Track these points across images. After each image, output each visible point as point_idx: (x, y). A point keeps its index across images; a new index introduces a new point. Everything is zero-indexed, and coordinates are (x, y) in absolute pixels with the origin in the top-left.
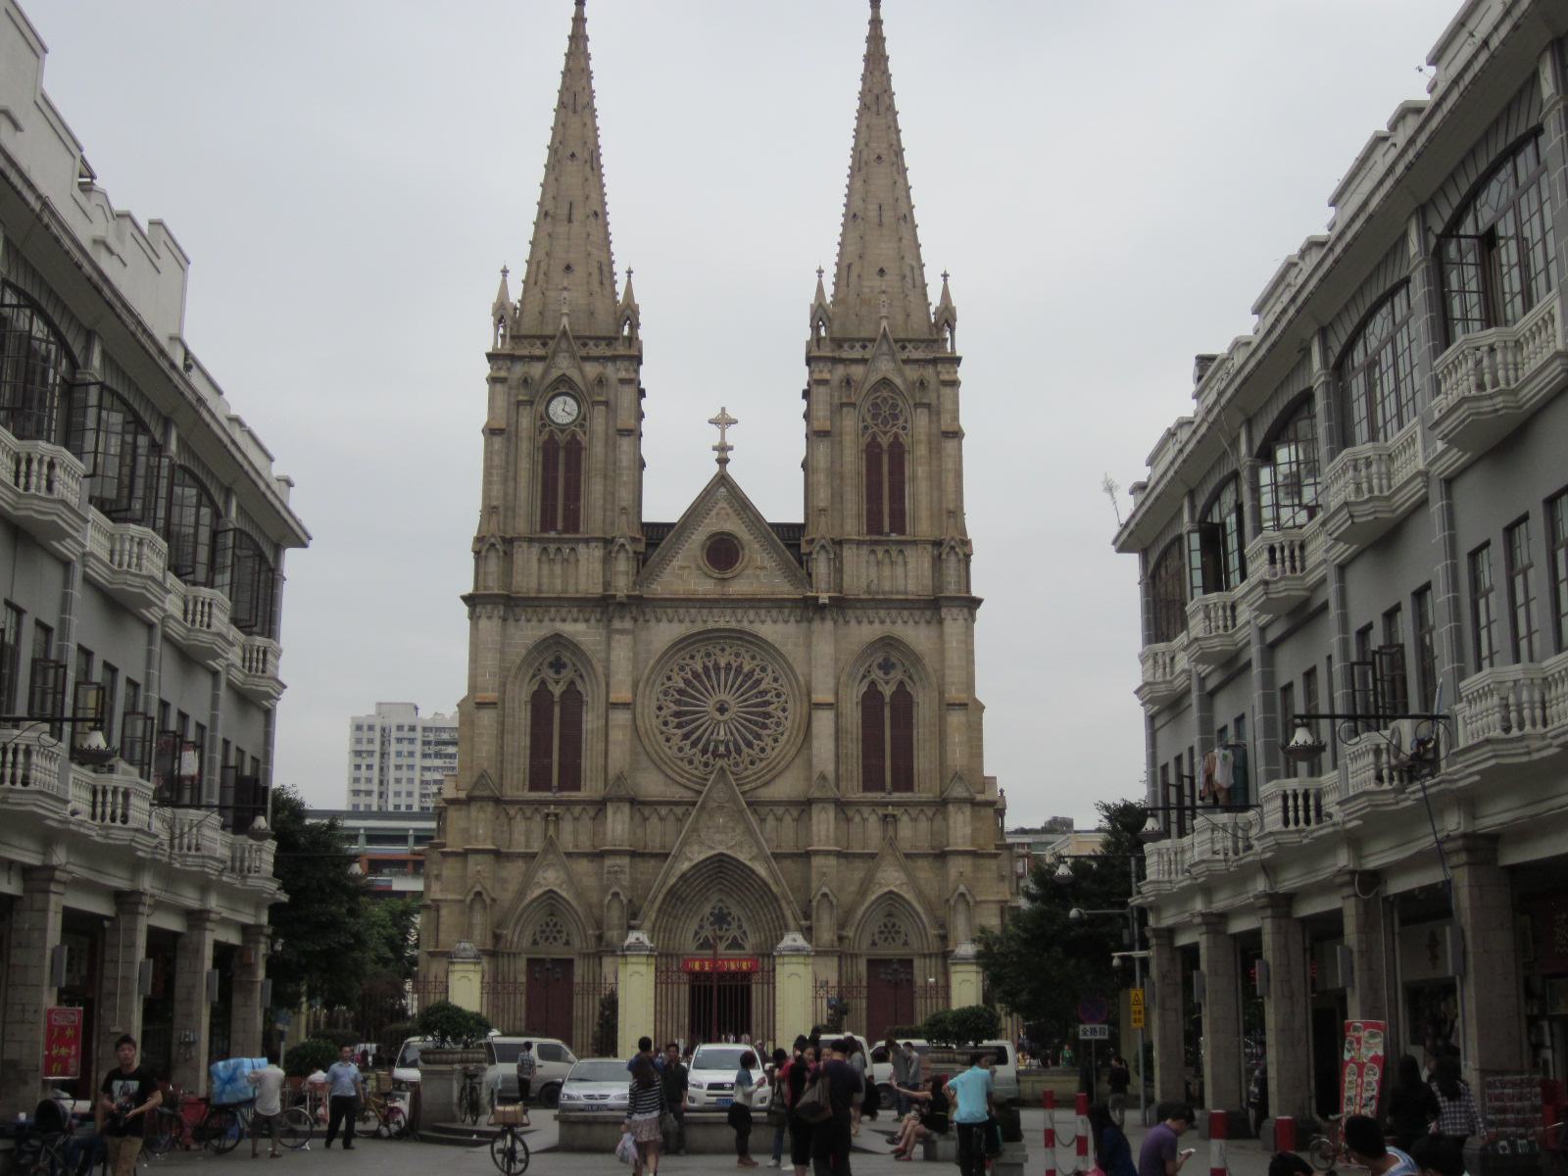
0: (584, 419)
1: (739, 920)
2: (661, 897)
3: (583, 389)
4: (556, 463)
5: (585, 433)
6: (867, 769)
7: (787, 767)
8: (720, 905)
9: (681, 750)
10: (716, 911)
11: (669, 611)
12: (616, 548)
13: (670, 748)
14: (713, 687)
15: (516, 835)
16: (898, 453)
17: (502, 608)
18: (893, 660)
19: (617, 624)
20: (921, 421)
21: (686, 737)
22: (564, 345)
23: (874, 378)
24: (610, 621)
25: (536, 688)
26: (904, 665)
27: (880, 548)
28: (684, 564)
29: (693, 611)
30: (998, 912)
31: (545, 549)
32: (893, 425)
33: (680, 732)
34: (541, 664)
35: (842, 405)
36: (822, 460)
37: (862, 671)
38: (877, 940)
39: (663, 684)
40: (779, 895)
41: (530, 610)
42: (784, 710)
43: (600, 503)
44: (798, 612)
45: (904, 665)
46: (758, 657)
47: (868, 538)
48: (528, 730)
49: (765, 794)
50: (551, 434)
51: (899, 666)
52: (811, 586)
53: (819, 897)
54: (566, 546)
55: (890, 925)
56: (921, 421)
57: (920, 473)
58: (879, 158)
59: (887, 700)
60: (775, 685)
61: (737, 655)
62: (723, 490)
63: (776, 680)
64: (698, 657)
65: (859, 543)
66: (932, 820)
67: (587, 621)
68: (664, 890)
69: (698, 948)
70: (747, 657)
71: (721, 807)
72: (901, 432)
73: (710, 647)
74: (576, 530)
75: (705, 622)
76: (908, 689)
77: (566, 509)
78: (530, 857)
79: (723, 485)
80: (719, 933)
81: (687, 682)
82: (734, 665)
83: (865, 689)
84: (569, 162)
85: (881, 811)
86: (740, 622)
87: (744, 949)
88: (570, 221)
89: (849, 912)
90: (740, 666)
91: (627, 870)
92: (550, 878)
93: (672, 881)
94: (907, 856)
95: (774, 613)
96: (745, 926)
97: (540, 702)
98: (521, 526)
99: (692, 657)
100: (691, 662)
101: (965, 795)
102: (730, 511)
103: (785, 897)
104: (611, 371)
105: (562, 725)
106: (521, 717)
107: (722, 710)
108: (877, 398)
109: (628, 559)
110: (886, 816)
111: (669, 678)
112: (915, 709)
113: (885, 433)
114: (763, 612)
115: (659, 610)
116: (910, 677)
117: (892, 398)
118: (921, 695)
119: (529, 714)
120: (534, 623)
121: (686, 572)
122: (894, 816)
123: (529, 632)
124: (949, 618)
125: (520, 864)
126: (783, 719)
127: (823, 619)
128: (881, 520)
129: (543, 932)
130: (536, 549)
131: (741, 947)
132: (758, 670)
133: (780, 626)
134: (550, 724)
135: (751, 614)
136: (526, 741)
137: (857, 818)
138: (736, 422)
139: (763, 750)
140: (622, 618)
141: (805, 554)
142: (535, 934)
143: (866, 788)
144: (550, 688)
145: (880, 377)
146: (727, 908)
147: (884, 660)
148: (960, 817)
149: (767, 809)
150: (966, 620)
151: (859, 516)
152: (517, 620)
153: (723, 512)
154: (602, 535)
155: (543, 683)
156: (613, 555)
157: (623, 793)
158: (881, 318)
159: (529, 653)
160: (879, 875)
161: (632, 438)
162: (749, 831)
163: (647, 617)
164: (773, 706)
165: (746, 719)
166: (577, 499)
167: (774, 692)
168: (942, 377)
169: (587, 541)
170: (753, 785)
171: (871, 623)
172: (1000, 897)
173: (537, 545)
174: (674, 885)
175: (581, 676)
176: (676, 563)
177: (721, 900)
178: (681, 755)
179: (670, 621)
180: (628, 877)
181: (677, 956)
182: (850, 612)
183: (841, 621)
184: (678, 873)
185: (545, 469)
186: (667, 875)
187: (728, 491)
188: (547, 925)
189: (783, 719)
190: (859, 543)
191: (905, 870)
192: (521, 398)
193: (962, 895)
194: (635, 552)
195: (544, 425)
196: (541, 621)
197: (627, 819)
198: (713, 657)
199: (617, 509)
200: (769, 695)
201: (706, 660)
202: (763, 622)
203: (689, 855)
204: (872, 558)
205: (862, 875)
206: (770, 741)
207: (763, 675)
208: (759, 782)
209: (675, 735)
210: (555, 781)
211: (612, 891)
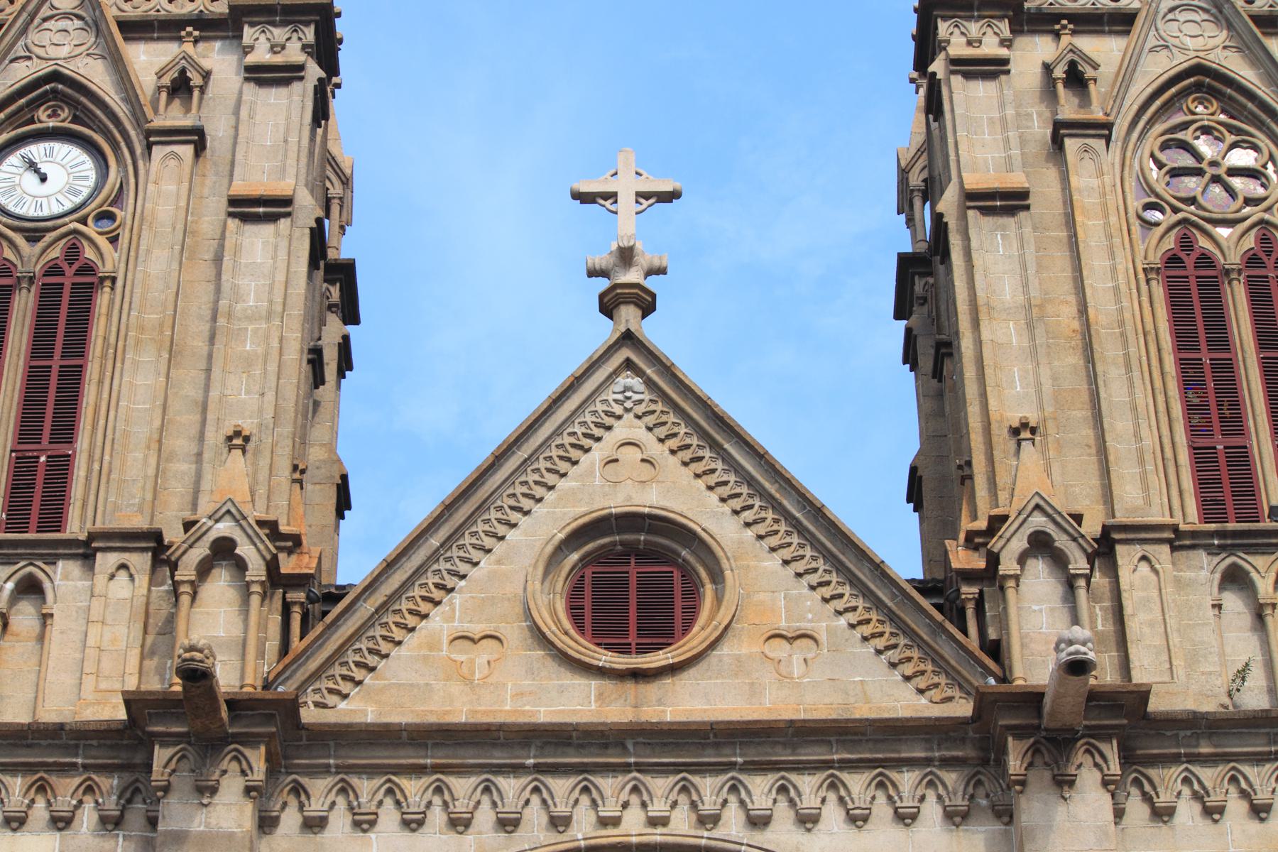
0: (118, 199)
3: (121, 109)
5: (114, 240)
11: (413, 788)
12: (201, 551)
23: (1157, 67)
24: (153, 822)
27: (1260, 561)
28: (477, 629)
29: (510, 786)
43: (143, 431)
44: (951, 777)
47: (1212, 527)
52: (1004, 679)
65: (1179, 540)
67: (61, 822)
74: (54, 517)
79: (628, 364)
86: (708, 820)
95: (857, 783)
102: (657, 451)
108: (1184, 126)
109: (245, 591)
114: (808, 785)
115: (366, 787)
117: (1232, 129)
127: (1064, 783)
135: (760, 788)
140: (206, 790)
141: (969, 576)
145: (1180, 62)
151: (1167, 464)
153: (631, 454)
154: (139, 522)
156: (186, 571)
161: (284, 223)
163: (316, 806)
166: (66, 430)
169: (85, 551)
176: (439, 623)
179: (413, 824)
182: (1168, 780)
183: (1136, 809)
187: (649, 383)
194: (272, 566)
199: (214, 437)
204: (1233, 602)
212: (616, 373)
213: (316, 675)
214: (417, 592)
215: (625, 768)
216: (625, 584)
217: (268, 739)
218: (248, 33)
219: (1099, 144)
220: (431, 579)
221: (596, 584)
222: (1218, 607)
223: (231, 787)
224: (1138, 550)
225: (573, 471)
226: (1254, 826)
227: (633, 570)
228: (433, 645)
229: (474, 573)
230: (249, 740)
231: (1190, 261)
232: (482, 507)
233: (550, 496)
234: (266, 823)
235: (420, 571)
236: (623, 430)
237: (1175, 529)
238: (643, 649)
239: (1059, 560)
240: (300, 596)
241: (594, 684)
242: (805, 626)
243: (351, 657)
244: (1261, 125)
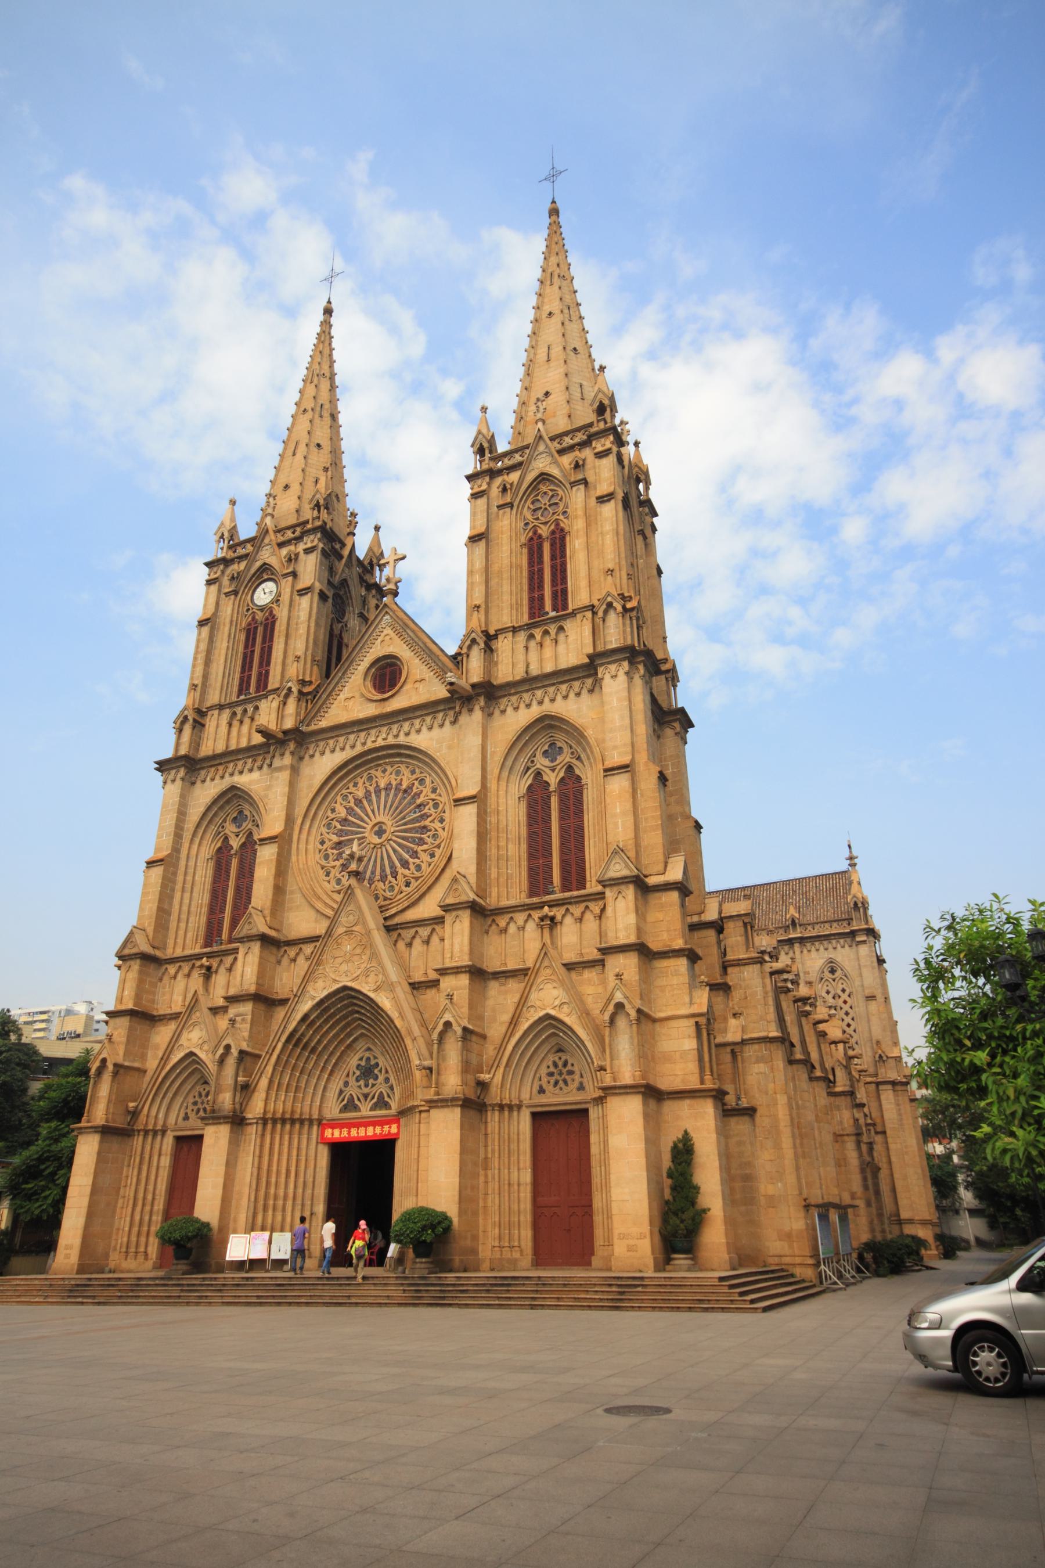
1: (387, 1072)
2: (280, 1046)
4: (254, 639)
6: (532, 873)
7: (437, 879)
8: (367, 1054)
9: (339, 881)
10: (363, 1063)
12: (285, 691)
13: (329, 882)
14: (373, 811)
15: (175, 997)
16: (559, 539)
17: (182, 772)
18: (559, 744)
19: (277, 763)
20: (577, 497)
21: (344, 866)
22: (266, 541)
23: (530, 477)
25: (219, 845)
26: (571, 747)
28: (350, 695)
30: (692, 1031)
31: (234, 714)
32: (554, 514)
33: (338, 863)
34: (225, 821)
35: (499, 507)
36: (479, 564)
37: (522, 762)
38: (544, 1086)
39: (327, 817)
40: (403, 1031)
41: (213, 769)
42: (442, 821)
45: (571, 747)
46: (417, 770)
48: (208, 886)
49: (412, 915)
50: (254, 618)
51: (566, 749)
53: (440, 1027)
54: (251, 705)
55: (560, 1064)
56: (577, 497)
57: (577, 545)
58: (550, 314)
59: (552, 788)
60: (433, 796)
61: (398, 773)
62: (387, 617)
63: (434, 790)
64: (360, 784)
66: (600, 917)
67: (260, 768)
68: (283, 1039)
69: (341, 1112)
70: (405, 772)
71: (349, 932)
72: (561, 517)
73: (373, 772)
75: (364, 744)
76: (577, 772)
77: (260, 674)
78: (175, 1016)
80: (366, 1090)
81: (350, 811)
82: (394, 783)
83: (529, 782)
84: (302, 416)
85: (536, 915)
86: (396, 736)
87: (390, 1108)
88: (294, 454)
89: (501, 1048)
90: (401, 784)
91: (249, 1018)
92: (194, 1039)
93: (291, 1027)
94: (569, 967)
96: (392, 1078)
97: (221, 858)
98: (214, 697)
99: (355, 785)
100: (352, 789)
101: (625, 872)
102: (393, 635)
103: (410, 1032)
104: (301, 547)
105: (240, 876)
106: (203, 874)
107: (380, 833)
108: (537, 495)
110: (542, 919)
111: (333, 810)
112: (585, 791)
113: (545, 523)
116: (579, 758)
117: (551, 490)
118: (589, 775)
119: (210, 872)
120: (217, 781)
121: (351, 703)
122: (552, 919)
123: (208, 790)
124: (607, 677)
125: (172, 1026)
126: (440, 830)
127: (471, 710)
128: (542, 606)
129: (195, 1103)
130: (226, 714)
131: (387, 1106)
132: (416, 783)
133: (436, 731)
134: (228, 880)
135: (406, 726)
136: (206, 898)
137: (512, 928)
138: (404, 558)
139: (418, 868)
140: (282, 755)
142: (187, 1108)
143: (531, 895)
144: (231, 842)
146: (375, 1058)
147: (550, 746)
148: (621, 903)
149: (413, 931)
150: (627, 673)
152: (204, 781)
153: (388, 638)
155: (226, 839)
157: (254, 932)
158: (536, 423)
159: (208, 809)
160: (533, 996)
161: (309, 594)
162: (374, 955)
164: (430, 819)
165: (403, 838)
166: (268, 664)
167: (431, 803)
168: (596, 451)
170: (400, 907)
171: (528, 706)
172: (695, 1009)
173: (228, 710)
174: (295, 1031)
175: (258, 826)
176: (342, 696)
177: (369, 1049)
178: (338, 888)
180: (248, 1026)
181: (311, 1121)
184: (299, 1016)
185: (246, 647)
186: (287, 1019)
187: (392, 617)
188: (200, 1095)
189: (440, 830)
190: (515, 630)
191: (562, 983)
192: (227, 590)
193: (620, 1006)
194: (300, 692)
195: (248, 610)
196: (222, 777)
197: (256, 960)
198: (375, 780)
200: (427, 807)
201: (367, 784)
202: (418, 731)
203: (312, 993)
204: (532, 644)
205: (516, 999)
206: (425, 857)
207: (421, 788)
208: (406, 904)
209: (334, 867)
210: (225, 936)
211: (225, 1043)
212: (384, 616)
213: (313, 717)
214: (337, 689)
215: (377, 727)
216: (385, 674)
217: (295, 739)
218: (305, 539)
219: (508, 510)
220: (340, 685)
221: (380, 675)
222: (527, 648)
223: (287, 755)
224: (504, 635)
225: (374, 646)
226: (527, 711)
227: (388, 670)
228: (340, 703)
229: (350, 680)
230: (289, 740)
231: (535, 538)
232: (351, 662)
233: (368, 655)
234: (301, 758)
235: (337, 683)
236: (385, 632)
237: (514, 627)
238: (389, 691)
239: (479, 644)
240: (309, 697)
241: (374, 704)
242: (423, 677)
243: (322, 710)
244: (560, 487)
